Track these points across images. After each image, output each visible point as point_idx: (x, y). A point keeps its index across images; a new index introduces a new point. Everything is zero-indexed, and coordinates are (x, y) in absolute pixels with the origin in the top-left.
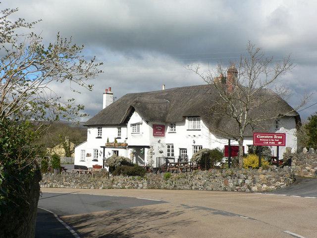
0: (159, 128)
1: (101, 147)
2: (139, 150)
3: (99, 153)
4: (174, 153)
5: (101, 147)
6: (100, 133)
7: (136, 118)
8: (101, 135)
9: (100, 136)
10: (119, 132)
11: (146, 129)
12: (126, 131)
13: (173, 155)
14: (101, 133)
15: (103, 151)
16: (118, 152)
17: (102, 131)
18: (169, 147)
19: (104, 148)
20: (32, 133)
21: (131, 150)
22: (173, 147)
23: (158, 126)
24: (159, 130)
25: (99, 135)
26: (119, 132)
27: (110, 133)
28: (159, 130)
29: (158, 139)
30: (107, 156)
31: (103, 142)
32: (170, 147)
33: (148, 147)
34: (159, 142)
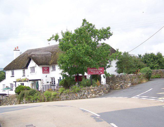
0: (46, 69)
1: (14, 82)
2: (35, 82)
3: (13, 85)
4: (55, 82)
5: (14, 82)
6: (13, 74)
7: (32, 64)
8: (14, 75)
9: (13, 76)
10: (24, 72)
11: (39, 69)
12: (28, 71)
13: (55, 83)
14: (14, 73)
15: (15, 84)
16: (23, 84)
17: (14, 73)
18: (52, 79)
19: (15, 82)
20: (55, 88)
21: (31, 82)
22: (54, 79)
23: (45, 67)
24: (46, 71)
25: (12, 75)
26: (24, 72)
27: (18, 73)
28: (46, 71)
29: (46, 75)
30: (17, 86)
31: (14, 79)
32: (53, 79)
33: (40, 80)
34: (46, 76)
